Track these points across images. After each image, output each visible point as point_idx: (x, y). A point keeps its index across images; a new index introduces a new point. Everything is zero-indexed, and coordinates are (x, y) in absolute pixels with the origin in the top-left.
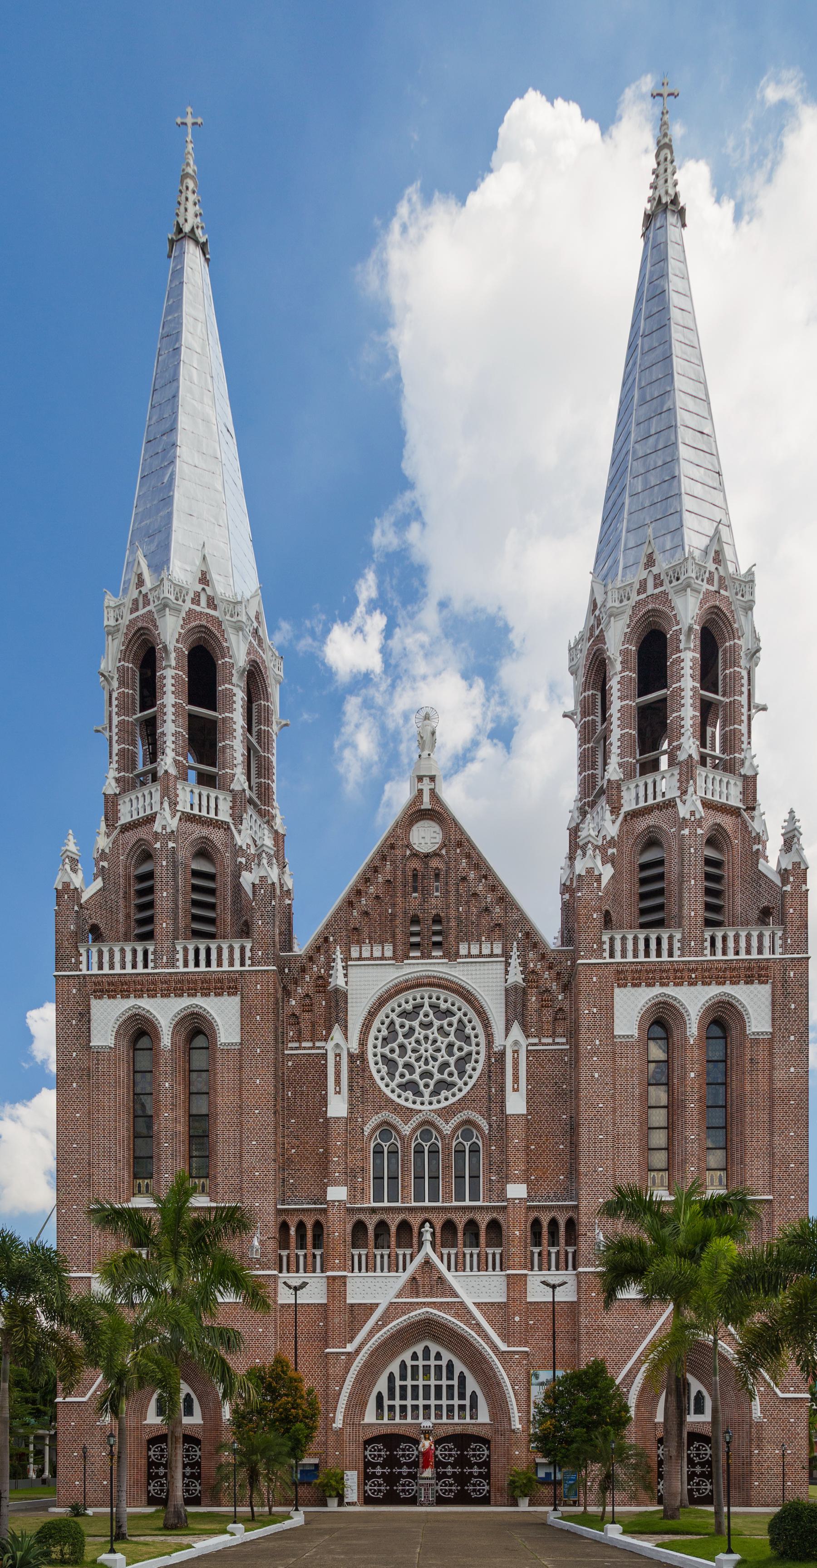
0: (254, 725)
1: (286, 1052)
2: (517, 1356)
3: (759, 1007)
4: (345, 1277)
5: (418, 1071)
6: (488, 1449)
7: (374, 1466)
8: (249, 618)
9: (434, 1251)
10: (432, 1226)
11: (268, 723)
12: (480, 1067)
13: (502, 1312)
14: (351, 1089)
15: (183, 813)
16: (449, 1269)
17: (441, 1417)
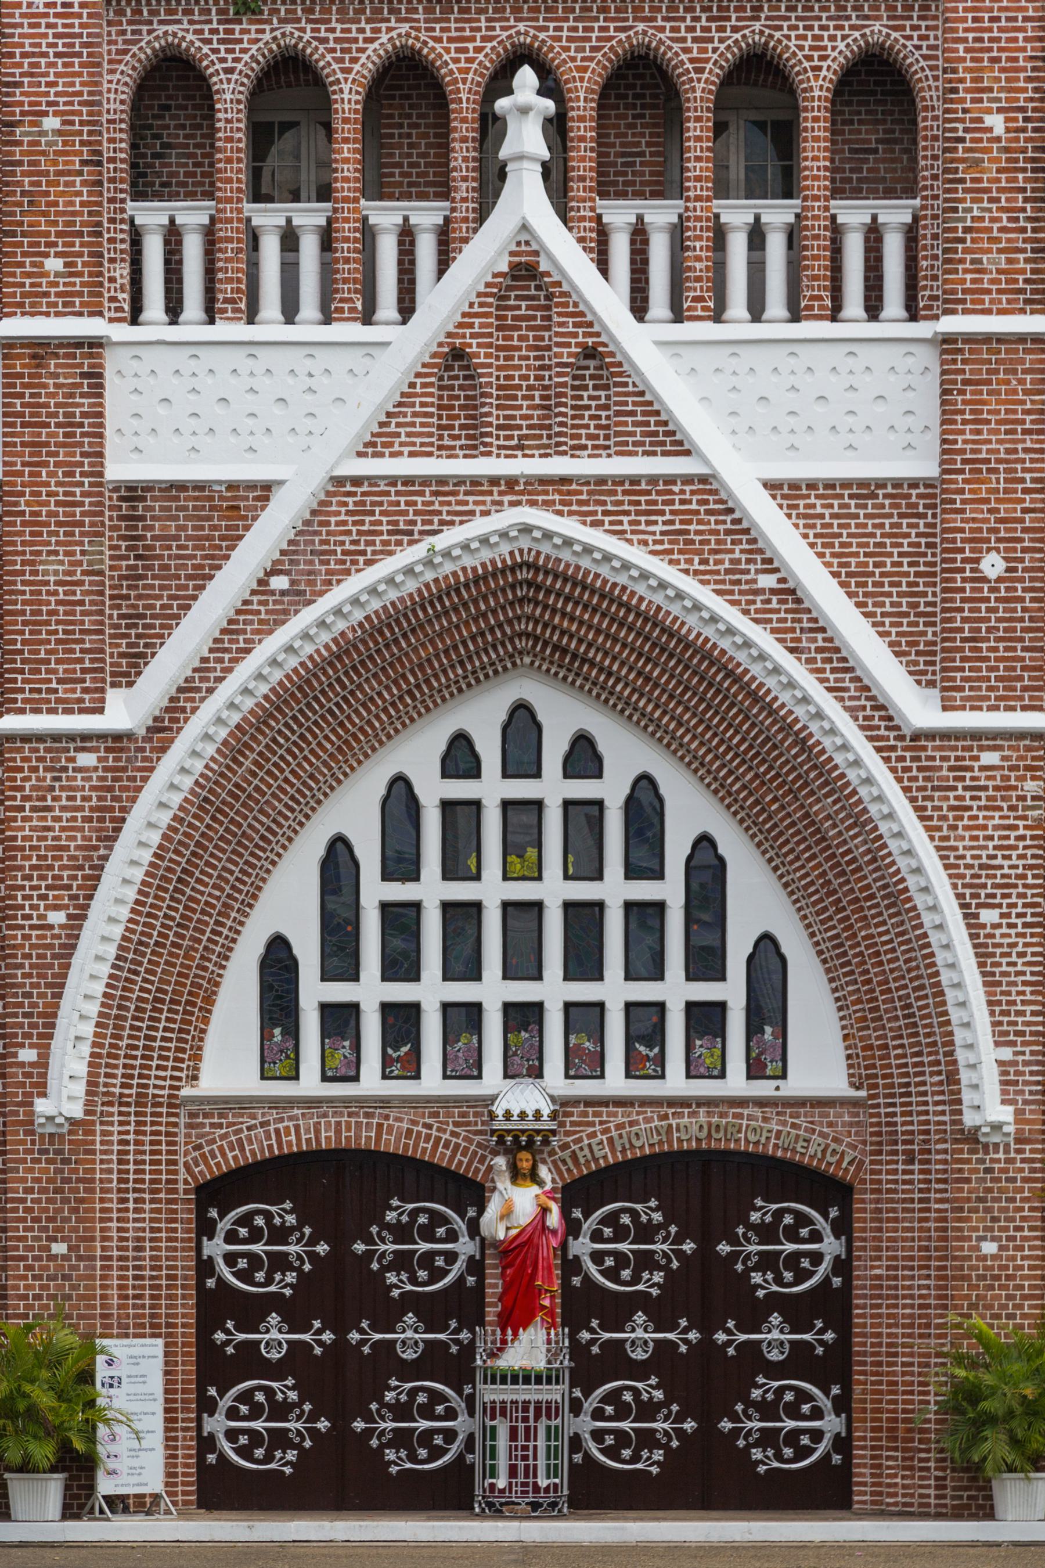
2: (990, 758)
4: (95, 345)
6: (842, 1228)
9: (563, 214)
13: (913, 532)
16: (639, 308)
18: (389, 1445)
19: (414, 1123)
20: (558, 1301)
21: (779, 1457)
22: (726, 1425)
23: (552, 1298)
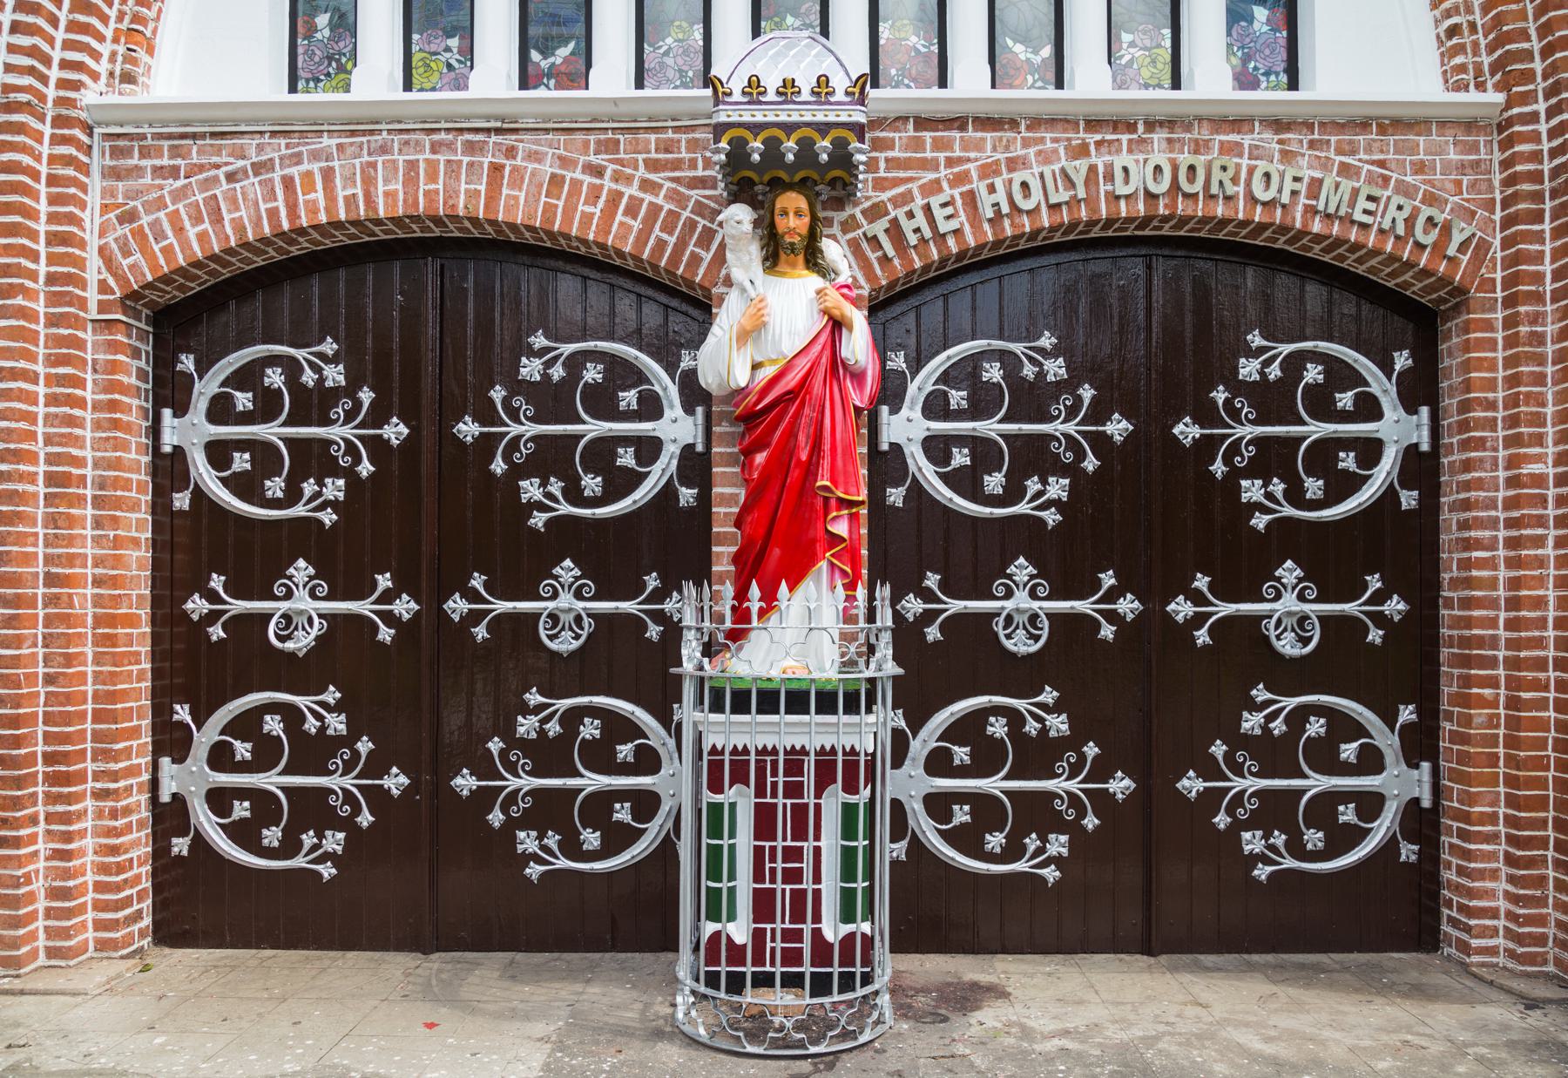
18: (526, 822)
19: (565, 162)
20: (864, 531)
21: (1015, 718)
22: (1192, 784)
23: (854, 518)
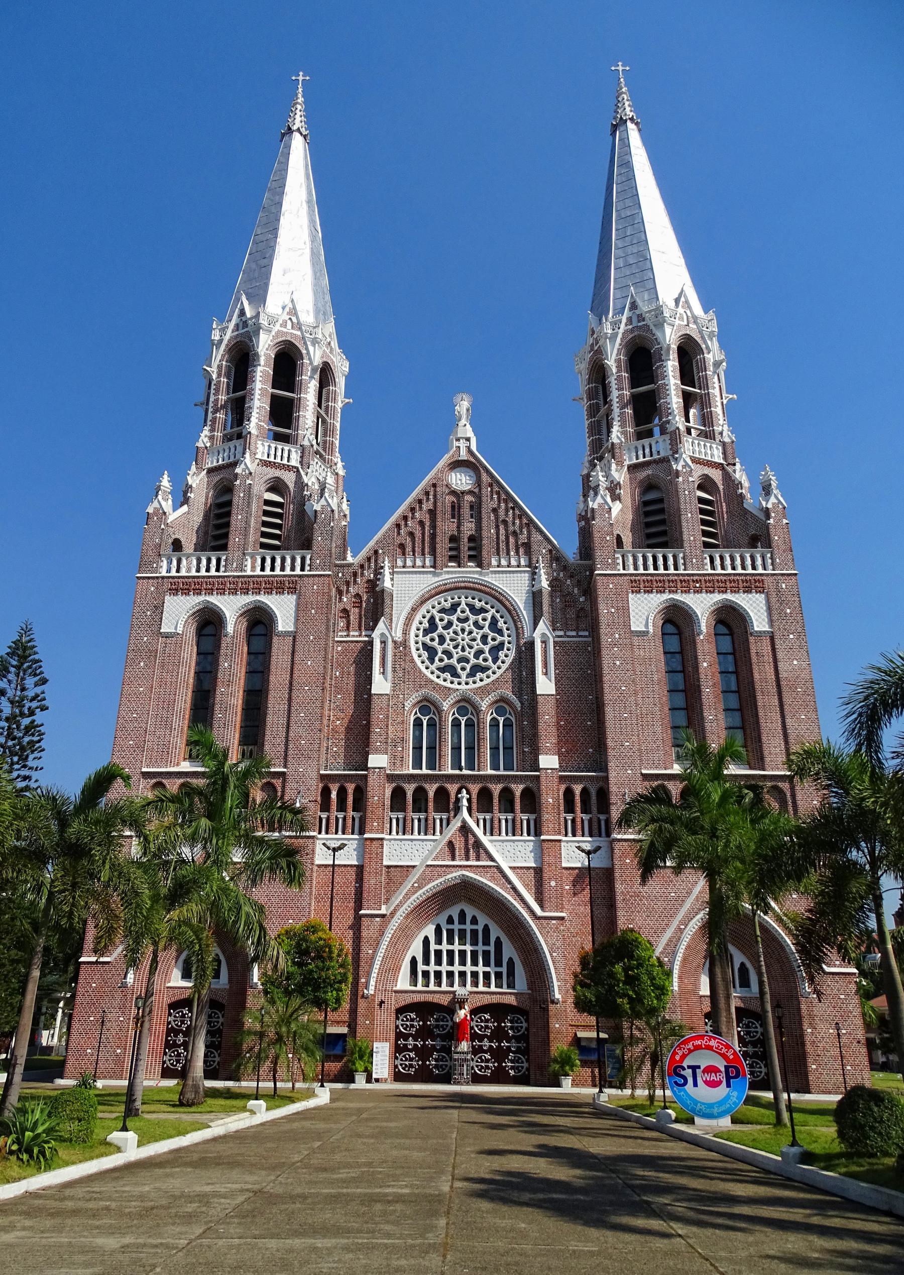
0: (323, 402)
1: (336, 639)
3: (759, 611)
5: (456, 656)
6: (527, 1021)
7: (406, 1037)
8: (324, 336)
9: (470, 815)
10: (468, 792)
11: (335, 400)
12: (512, 654)
14: (394, 671)
15: (261, 460)
16: (485, 834)
17: (477, 986)
